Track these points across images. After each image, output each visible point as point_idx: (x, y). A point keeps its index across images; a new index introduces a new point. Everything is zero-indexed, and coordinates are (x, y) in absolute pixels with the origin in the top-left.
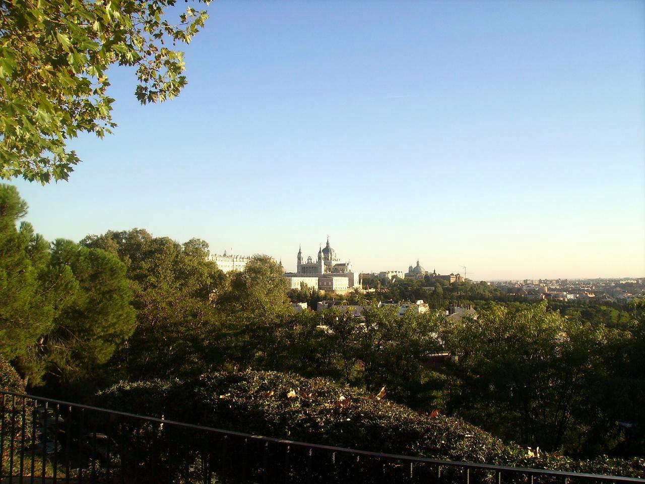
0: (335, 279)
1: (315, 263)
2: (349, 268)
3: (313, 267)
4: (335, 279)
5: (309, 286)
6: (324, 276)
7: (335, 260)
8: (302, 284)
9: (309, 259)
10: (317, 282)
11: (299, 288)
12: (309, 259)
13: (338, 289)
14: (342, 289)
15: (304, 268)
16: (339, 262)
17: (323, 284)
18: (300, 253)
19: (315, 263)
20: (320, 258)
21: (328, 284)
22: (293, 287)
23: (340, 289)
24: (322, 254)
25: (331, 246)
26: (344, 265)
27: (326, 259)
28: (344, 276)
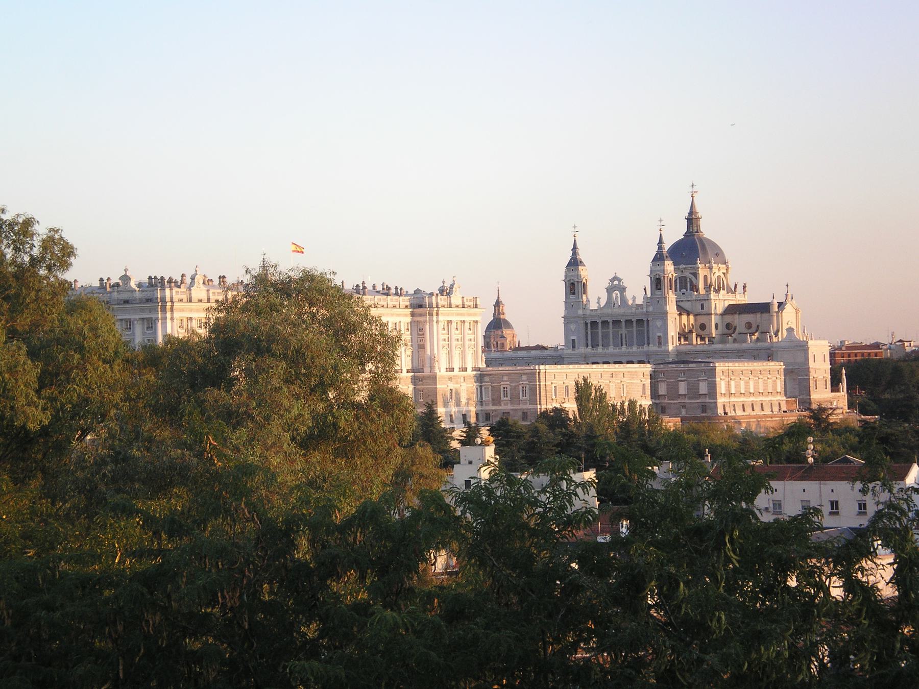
0: (721, 367)
1: (640, 301)
2: (788, 318)
3: (628, 322)
4: (721, 367)
5: (615, 396)
6: (682, 358)
7: (730, 291)
8: (583, 392)
9: (616, 286)
10: (648, 382)
11: (571, 407)
12: (616, 286)
13: (739, 413)
14: (758, 411)
15: (594, 324)
16: (740, 299)
17: (673, 392)
18: (574, 263)
19: (640, 301)
20: (657, 283)
21: (693, 392)
22: (547, 404)
23: (749, 411)
24: (669, 266)
25: (707, 230)
26: (763, 308)
27: (686, 284)
28: (769, 355)
